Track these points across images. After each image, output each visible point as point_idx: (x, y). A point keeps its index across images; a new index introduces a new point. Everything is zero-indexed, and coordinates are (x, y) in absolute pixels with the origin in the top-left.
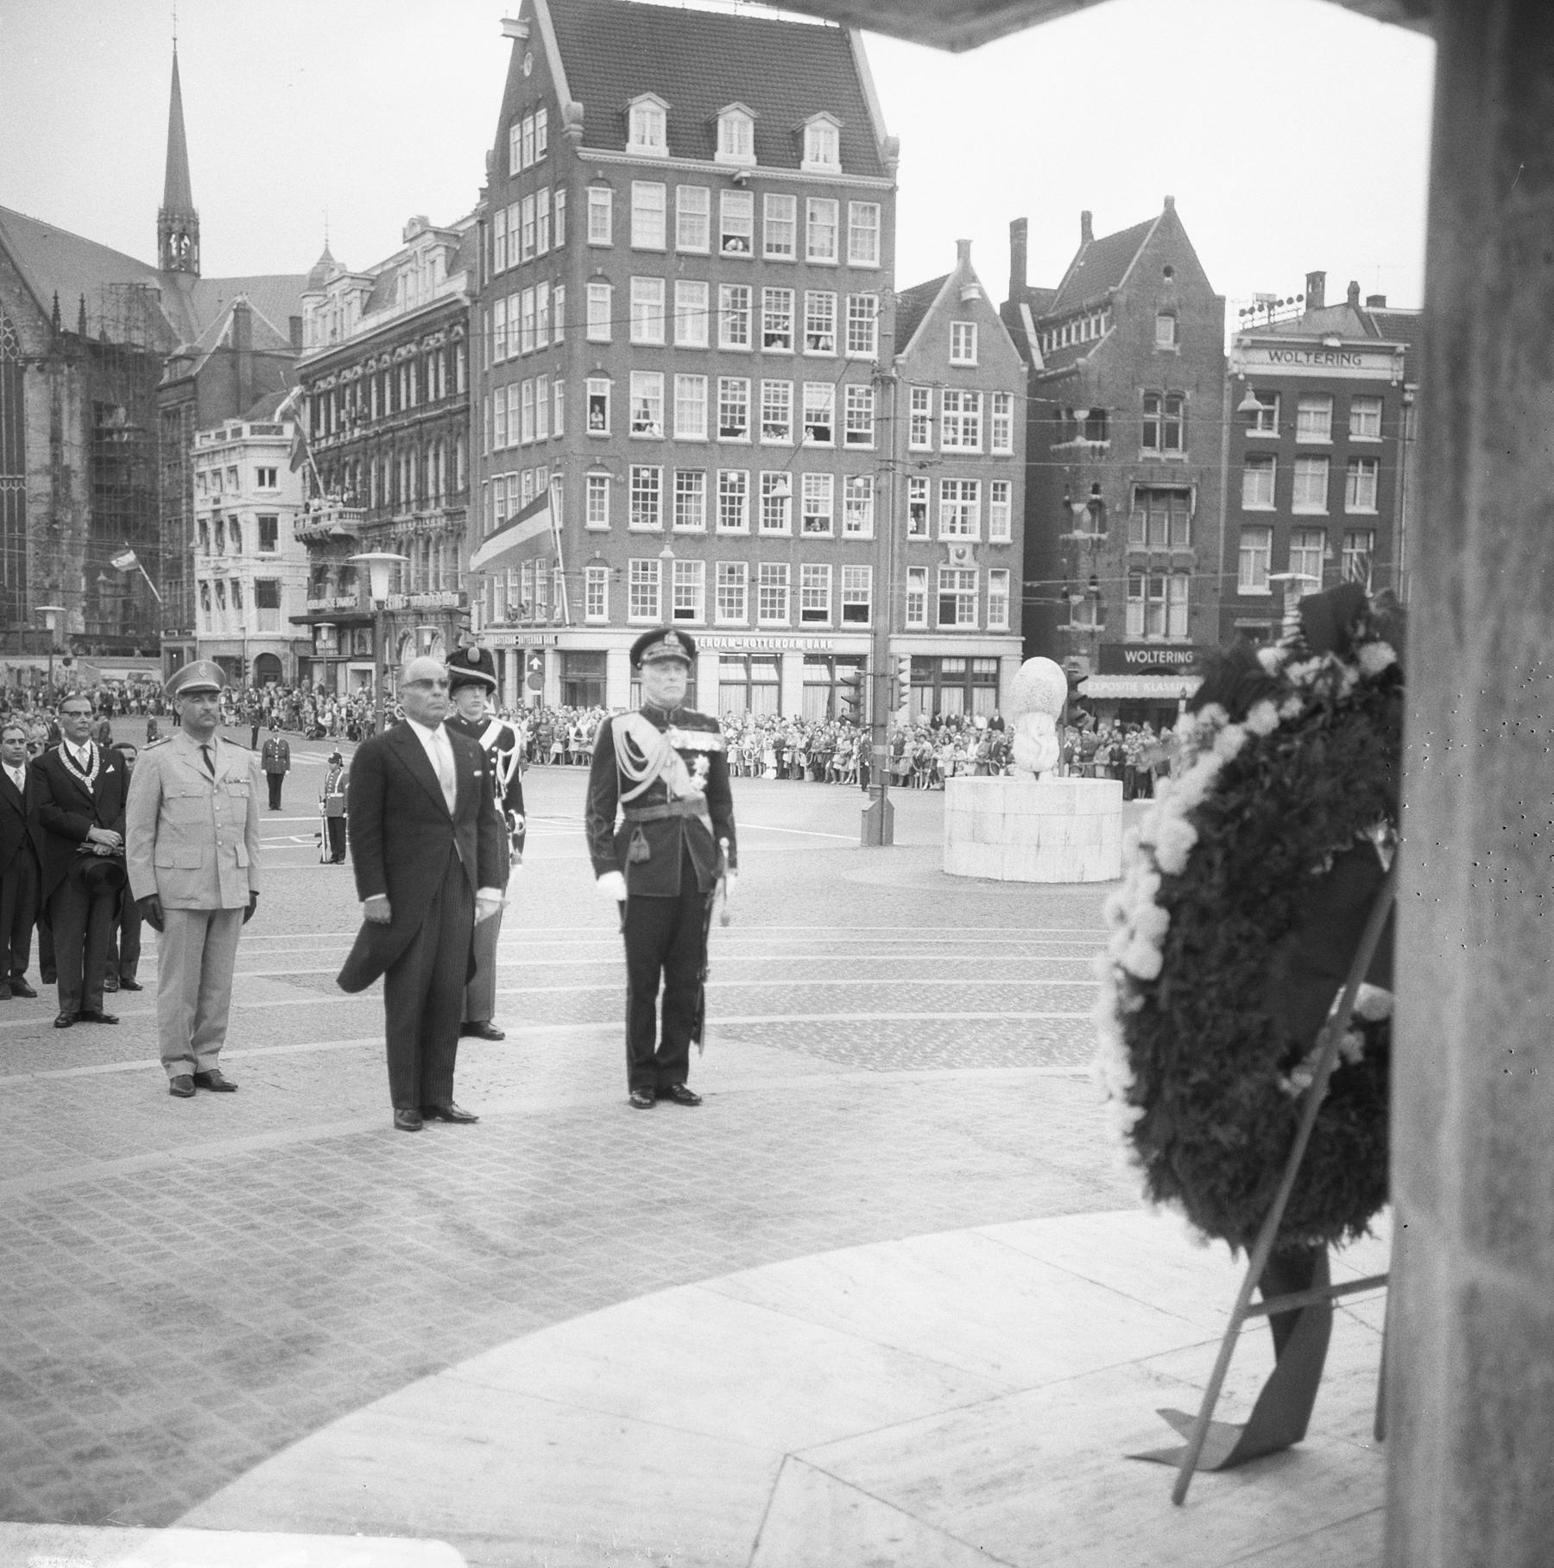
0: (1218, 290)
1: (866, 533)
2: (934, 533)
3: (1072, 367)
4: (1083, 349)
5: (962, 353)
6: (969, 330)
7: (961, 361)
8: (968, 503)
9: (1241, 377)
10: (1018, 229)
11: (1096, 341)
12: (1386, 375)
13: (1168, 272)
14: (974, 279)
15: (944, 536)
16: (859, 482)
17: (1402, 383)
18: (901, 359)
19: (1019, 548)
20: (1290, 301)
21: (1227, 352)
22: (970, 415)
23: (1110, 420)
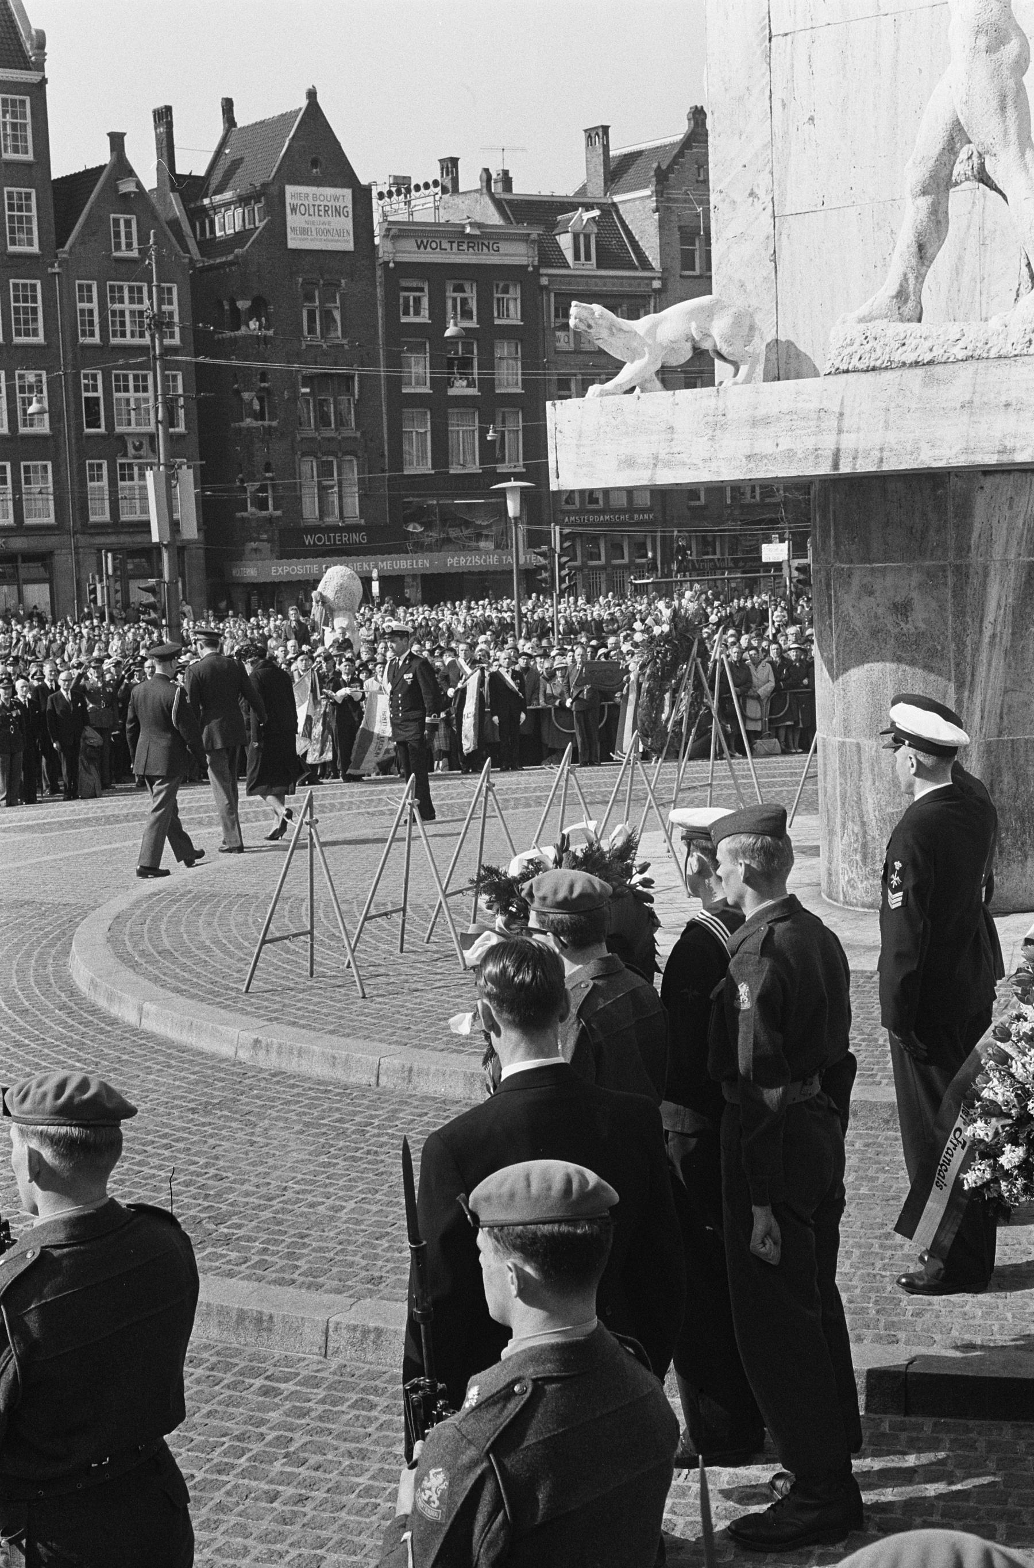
0: (364, 181)
1: (43, 427)
2: (110, 425)
3: (231, 257)
4: (240, 238)
5: (124, 247)
6: (128, 223)
7: (124, 253)
8: (141, 395)
9: (391, 265)
10: (164, 116)
11: (251, 231)
12: (523, 261)
13: (315, 163)
14: (131, 173)
15: (119, 429)
16: (31, 377)
17: (536, 268)
18: (64, 252)
19: (194, 438)
20: (427, 186)
21: (377, 241)
22: (136, 307)
23: (271, 309)
